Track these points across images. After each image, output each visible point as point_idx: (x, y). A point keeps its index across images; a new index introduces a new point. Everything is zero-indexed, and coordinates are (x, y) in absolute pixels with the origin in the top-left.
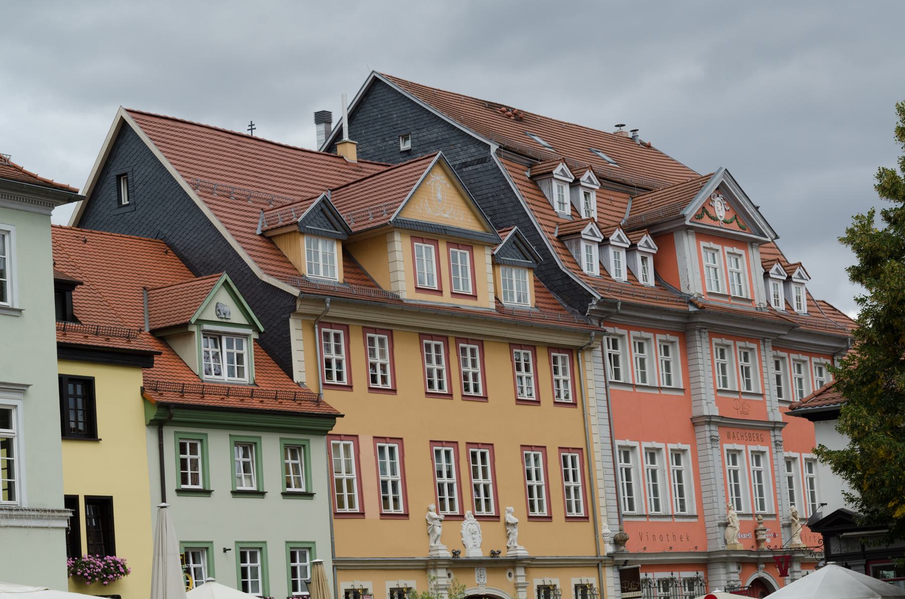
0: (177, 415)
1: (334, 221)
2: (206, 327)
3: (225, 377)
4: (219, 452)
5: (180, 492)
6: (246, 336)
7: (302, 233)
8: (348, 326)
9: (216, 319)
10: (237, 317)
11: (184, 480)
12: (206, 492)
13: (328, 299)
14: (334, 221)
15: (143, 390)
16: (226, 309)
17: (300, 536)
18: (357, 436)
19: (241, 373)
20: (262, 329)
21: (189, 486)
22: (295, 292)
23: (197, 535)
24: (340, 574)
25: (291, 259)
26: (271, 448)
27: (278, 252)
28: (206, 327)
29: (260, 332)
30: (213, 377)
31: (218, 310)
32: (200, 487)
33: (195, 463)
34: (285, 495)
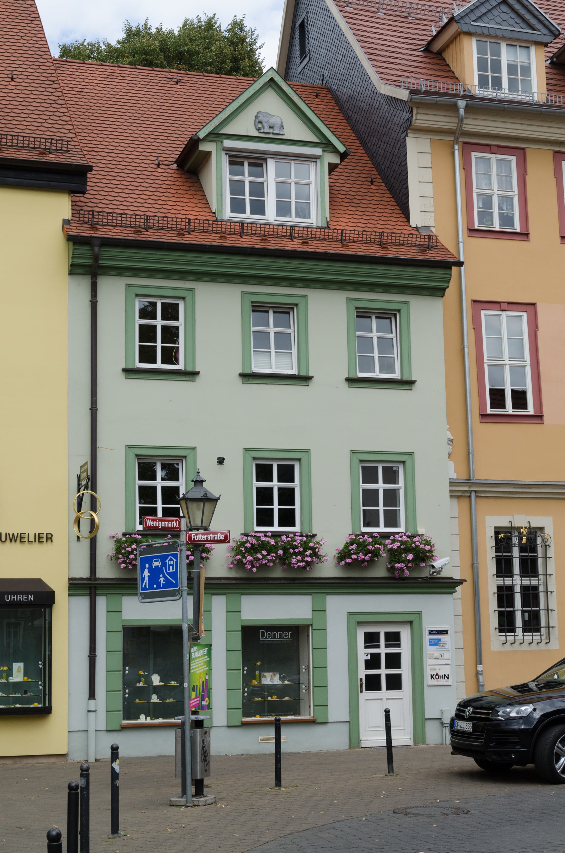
0: (111, 257)
1: (528, 16)
2: (228, 143)
3: (271, 215)
4: (215, 317)
5: (129, 372)
6: (314, 158)
7: (469, 34)
8: (523, 149)
9: (256, 134)
10: (295, 129)
11: (147, 355)
12: (191, 375)
13: (462, 104)
14: (528, 16)
15: (66, 222)
16: (273, 120)
17: (383, 441)
18: (534, 305)
19: (303, 212)
20: (342, 149)
21: (159, 365)
22: (403, 95)
23: (160, 437)
24: (481, 506)
25: (457, 75)
26: (327, 314)
27: (447, 68)
28: (228, 143)
29: (343, 156)
30: (248, 216)
31: (258, 122)
32: (180, 367)
33: (171, 334)
34: (352, 381)
